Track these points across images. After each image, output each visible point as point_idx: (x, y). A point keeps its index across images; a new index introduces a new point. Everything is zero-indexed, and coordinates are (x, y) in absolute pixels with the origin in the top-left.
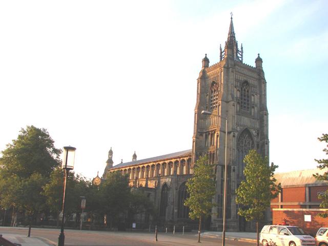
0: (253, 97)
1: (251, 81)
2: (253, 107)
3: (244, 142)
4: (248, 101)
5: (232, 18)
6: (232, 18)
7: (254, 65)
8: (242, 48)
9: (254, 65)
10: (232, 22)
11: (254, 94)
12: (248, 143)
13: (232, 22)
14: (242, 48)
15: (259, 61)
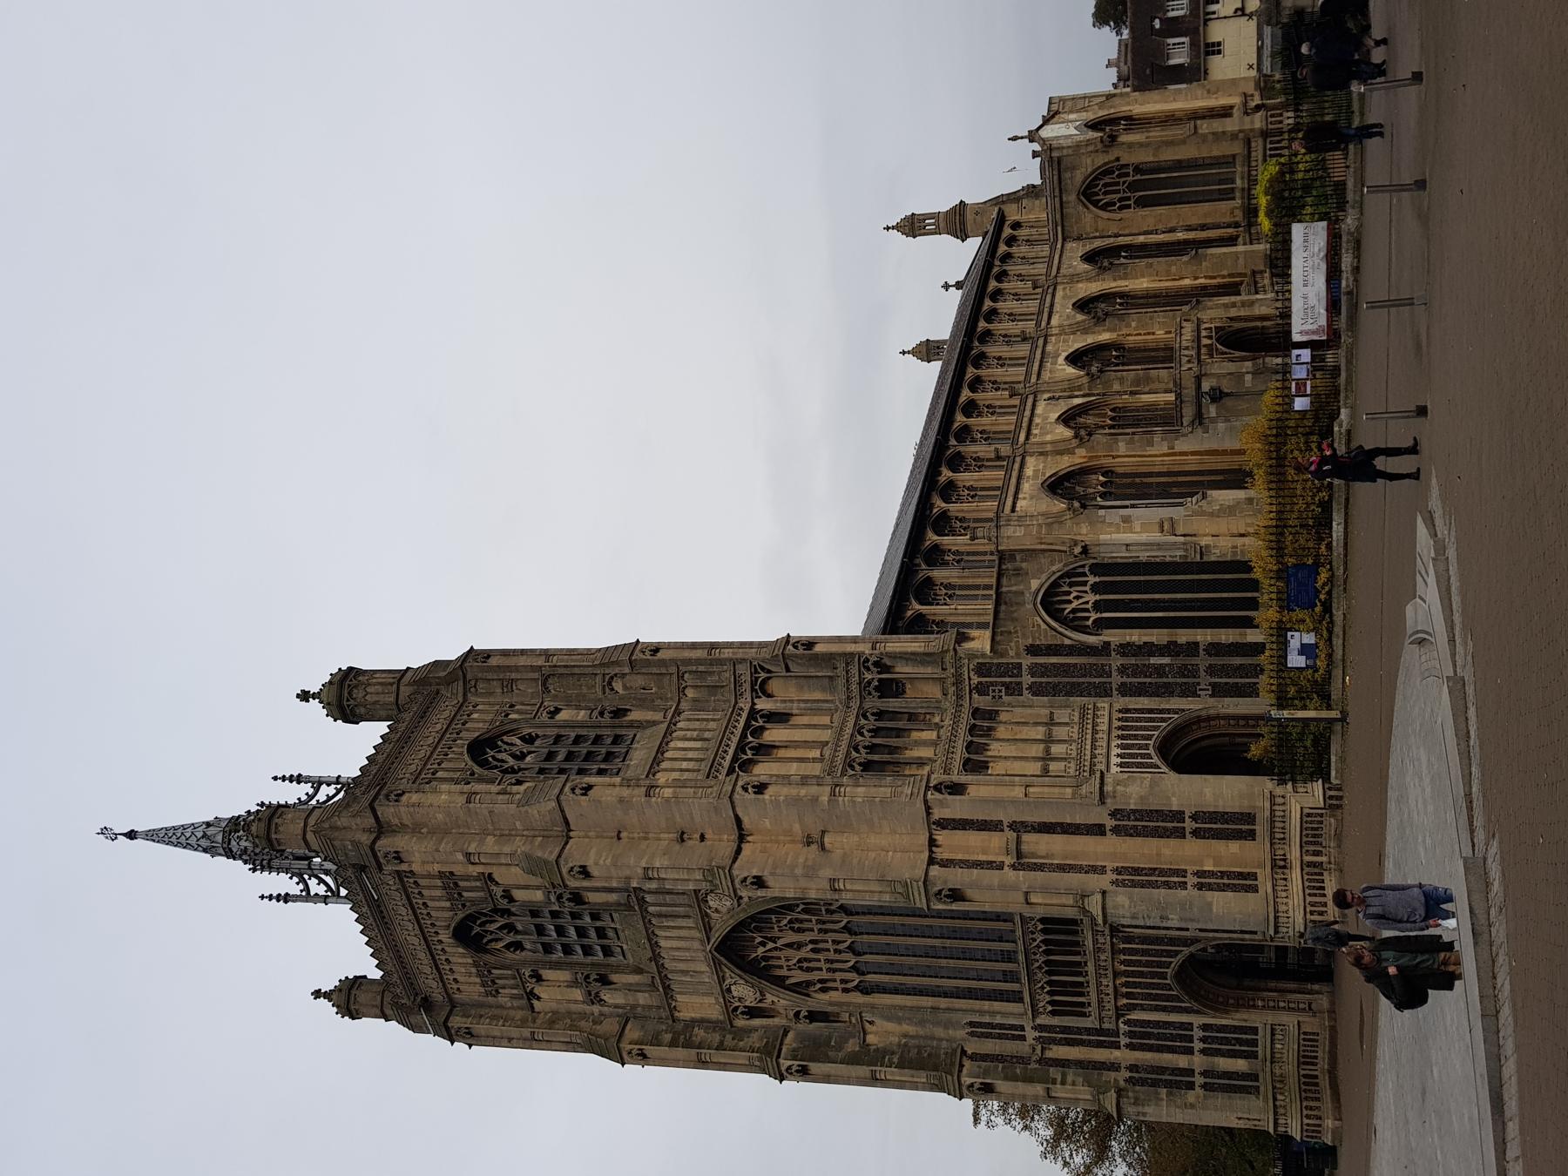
0: (518, 895)
1: (479, 723)
2: (577, 898)
3: (805, 953)
4: (555, 915)
5: (131, 835)
6: (131, 835)
7: (372, 733)
8: (299, 779)
9: (372, 733)
10: (153, 836)
11: (498, 891)
12: (800, 930)
13: (153, 836)
14: (299, 779)
15: (347, 695)
